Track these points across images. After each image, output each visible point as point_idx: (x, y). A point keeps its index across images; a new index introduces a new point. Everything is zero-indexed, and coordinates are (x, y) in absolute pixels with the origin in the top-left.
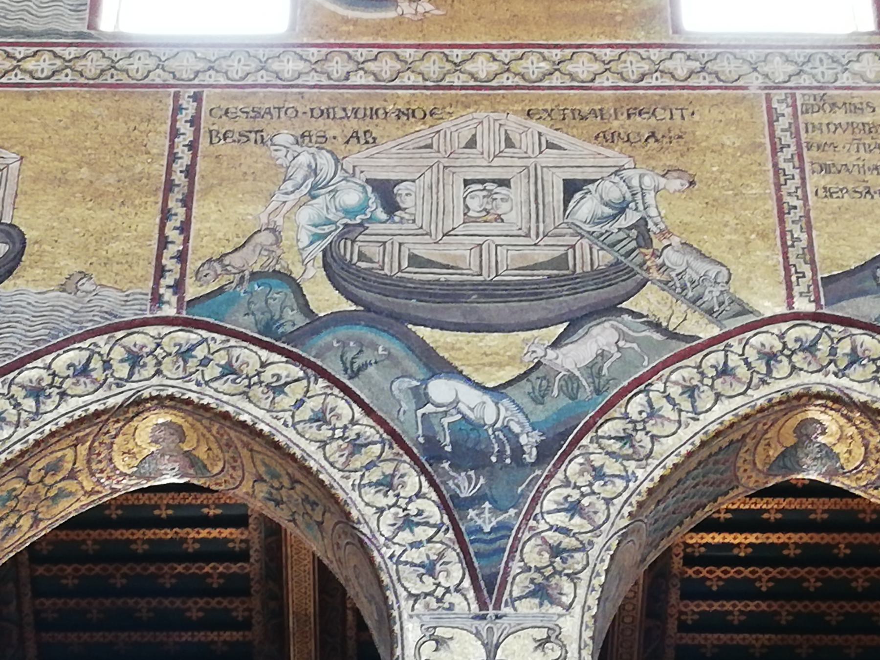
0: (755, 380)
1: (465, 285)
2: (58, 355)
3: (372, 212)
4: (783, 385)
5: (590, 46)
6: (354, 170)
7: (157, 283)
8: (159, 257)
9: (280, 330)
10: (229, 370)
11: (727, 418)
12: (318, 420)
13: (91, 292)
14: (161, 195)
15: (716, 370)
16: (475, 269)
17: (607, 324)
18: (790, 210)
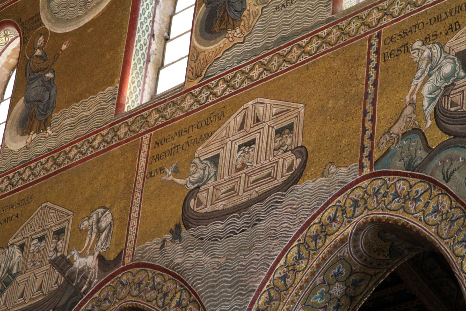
2: (323, 214)
3: (457, 74)
6: (450, 51)
9: (416, 164)
12: (435, 212)
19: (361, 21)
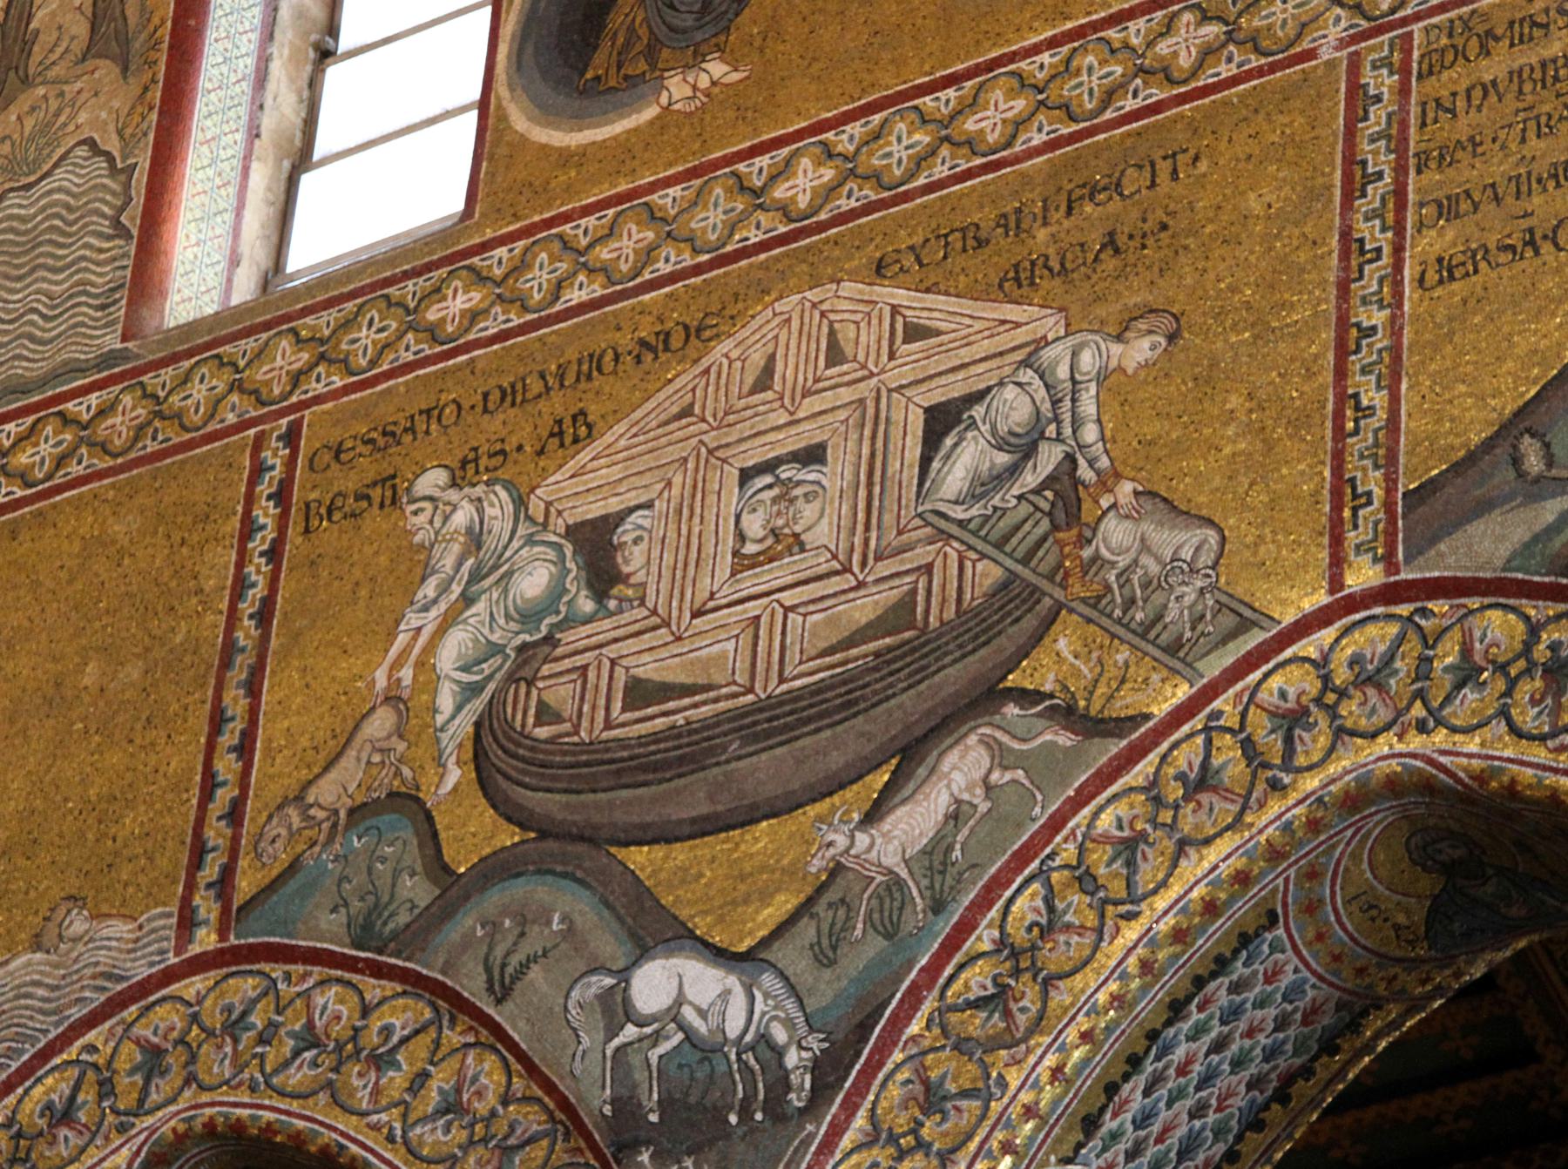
1: (718, 724)
2: (26, 1092)
3: (569, 603)
4: (1311, 783)
9: (391, 926)
11: (1195, 894)
12: (447, 1111)
13: (81, 938)
17: (972, 739)
19: (227, 375)
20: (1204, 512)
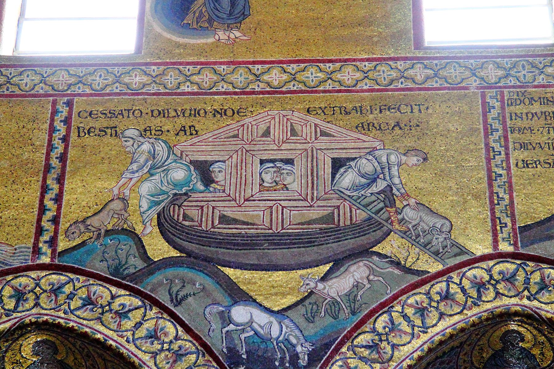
0: (469, 303)
1: (258, 237)
4: (489, 306)
5: (354, 60)
6: (181, 155)
7: (37, 239)
8: (39, 220)
10: (89, 302)
11: (448, 331)
12: (151, 337)
14: (41, 175)
15: (441, 296)
16: (267, 224)
17: (361, 264)
18: (496, 177)
20: (443, 215)
